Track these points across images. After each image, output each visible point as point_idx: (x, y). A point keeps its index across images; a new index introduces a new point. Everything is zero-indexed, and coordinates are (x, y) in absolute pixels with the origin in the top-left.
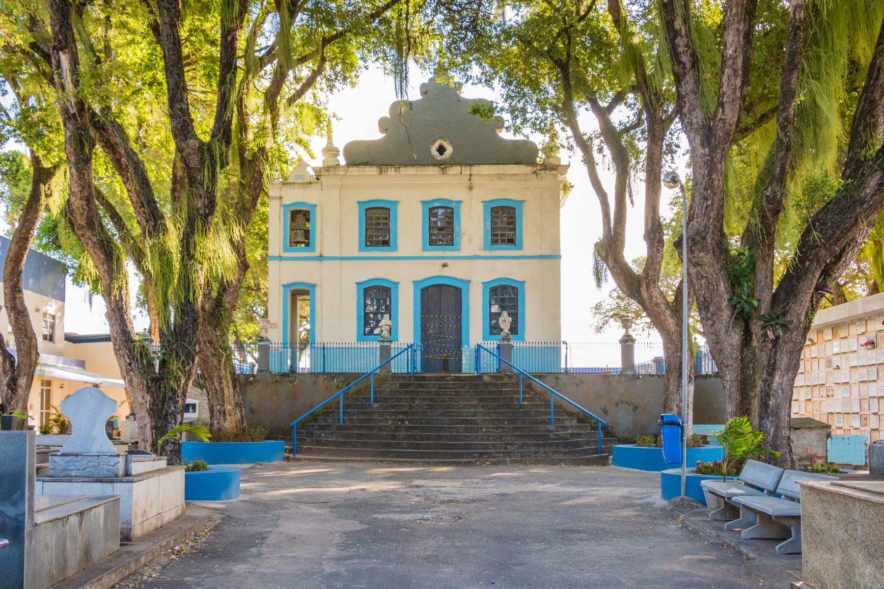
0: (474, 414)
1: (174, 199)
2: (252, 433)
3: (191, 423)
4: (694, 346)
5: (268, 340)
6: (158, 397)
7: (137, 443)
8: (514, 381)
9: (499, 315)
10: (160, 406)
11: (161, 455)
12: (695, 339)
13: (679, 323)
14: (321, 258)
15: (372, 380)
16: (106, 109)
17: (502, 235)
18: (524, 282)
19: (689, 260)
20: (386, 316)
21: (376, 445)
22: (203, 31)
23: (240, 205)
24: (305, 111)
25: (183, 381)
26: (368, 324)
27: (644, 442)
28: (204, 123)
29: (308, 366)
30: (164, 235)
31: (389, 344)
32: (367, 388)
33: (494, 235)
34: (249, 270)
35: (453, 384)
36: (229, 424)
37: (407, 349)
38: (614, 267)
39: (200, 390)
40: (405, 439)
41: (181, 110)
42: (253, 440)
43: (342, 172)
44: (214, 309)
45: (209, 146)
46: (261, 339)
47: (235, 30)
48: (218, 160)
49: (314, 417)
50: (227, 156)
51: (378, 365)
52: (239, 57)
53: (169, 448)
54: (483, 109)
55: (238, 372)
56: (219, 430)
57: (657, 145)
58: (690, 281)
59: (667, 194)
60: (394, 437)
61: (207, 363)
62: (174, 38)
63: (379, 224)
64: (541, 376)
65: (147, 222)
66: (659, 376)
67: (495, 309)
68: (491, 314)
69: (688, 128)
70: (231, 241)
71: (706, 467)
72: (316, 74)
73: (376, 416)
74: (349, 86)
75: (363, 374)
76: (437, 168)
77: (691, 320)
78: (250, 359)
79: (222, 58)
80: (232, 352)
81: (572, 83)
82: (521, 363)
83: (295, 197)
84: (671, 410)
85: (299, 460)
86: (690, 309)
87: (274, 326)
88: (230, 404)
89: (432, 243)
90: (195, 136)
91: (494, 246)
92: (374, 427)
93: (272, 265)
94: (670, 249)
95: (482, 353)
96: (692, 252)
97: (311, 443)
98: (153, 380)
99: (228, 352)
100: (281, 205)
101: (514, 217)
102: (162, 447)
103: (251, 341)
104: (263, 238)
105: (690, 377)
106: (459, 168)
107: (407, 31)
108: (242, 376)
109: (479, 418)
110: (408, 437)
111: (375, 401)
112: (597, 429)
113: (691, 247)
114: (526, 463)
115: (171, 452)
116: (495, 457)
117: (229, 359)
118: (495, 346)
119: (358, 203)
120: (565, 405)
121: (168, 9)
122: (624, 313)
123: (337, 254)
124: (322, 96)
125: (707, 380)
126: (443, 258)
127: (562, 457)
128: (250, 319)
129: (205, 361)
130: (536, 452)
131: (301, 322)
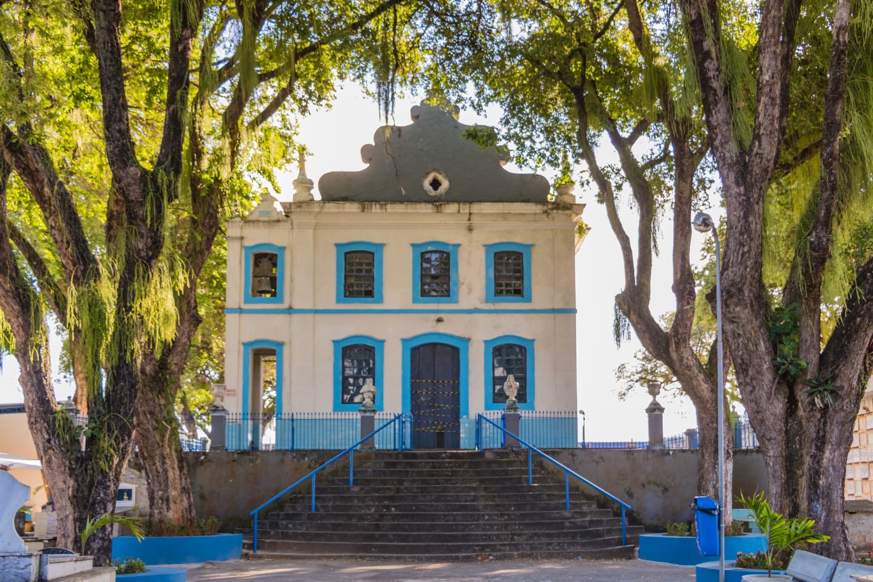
0: (475, 499)
1: (110, 238)
2: (202, 525)
3: (125, 514)
4: (731, 416)
5: (224, 410)
6: (83, 481)
7: (55, 539)
8: (522, 458)
9: (502, 380)
10: (86, 493)
11: (86, 553)
12: (734, 407)
13: (714, 390)
14: (290, 310)
15: (351, 458)
16: (26, 129)
17: (507, 285)
18: (533, 340)
19: (724, 315)
20: (369, 381)
21: (355, 537)
22: (148, 39)
23: (191, 246)
24: (272, 136)
25: (116, 461)
26: (346, 390)
27: (676, 531)
28: (148, 146)
29: (273, 442)
30: (95, 281)
31: (372, 414)
32: (346, 467)
33: (497, 285)
34: (201, 325)
35: (449, 463)
36: (173, 514)
37: (394, 420)
38: (638, 323)
39: (137, 473)
40: (391, 530)
41: (119, 131)
42: (203, 533)
43: (316, 209)
44: (157, 373)
45: (154, 175)
46: (216, 409)
47: (187, 39)
48: (165, 193)
49: (280, 504)
50: (176, 188)
51: (359, 440)
52: (193, 71)
53: (96, 545)
54: (483, 136)
55: (186, 450)
56: (161, 521)
57: (686, 182)
58: (726, 341)
59: (698, 239)
60: (377, 527)
61: (147, 438)
62: (112, 46)
63: (360, 271)
64: (554, 453)
65: (74, 265)
66: (692, 452)
67: (500, 372)
68: (494, 378)
69: (721, 165)
70: (175, 293)
71: (748, 560)
72: (284, 93)
73: (356, 502)
74: (325, 108)
75: (340, 451)
76: (430, 206)
77: (728, 386)
78: (201, 434)
79: (170, 71)
80: (179, 425)
81: (588, 110)
82: (531, 438)
83: (257, 237)
84: (707, 491)
85: (260, 557)
86: (726, 373)
87: (232, 393)
88: (175, 489)
89: (424, 293)
90: (136, 163)
91: (498, 298)
92: (354, 515)
93: (230, 319)
94: (702, 302)
95: (484, 425)
96: (727, 306)
97: (276, 536)
98: (77, 460)
99: (174, 425)
100: (242, 247)
101: (521, 264)
102: (88, 543)
103: (202, 411)
104: (218, 286)
105: (728, 453)
106: (456, 206)
107: (394, 44)
108: (191, 454)
109: (481, 503)
110: (395, 528)
111: (354, 484)
112: (620, 515)
113: (726, 300)
114: (536, 557)
115: (99, 550)
116: (500, 550)
117: (175, 434)
118: (500, 416)
119: (336, 245)
120: (582, 487)
121: (105, 12)
122: (650, 377)
123: (310, 306)
124: (292, 118)
125: (748, 457)
126: (437, 311)
127: (579, 549)
128: (202, 383)
129: (144, 436)
130: (549, 544)
131: (265, 387)
